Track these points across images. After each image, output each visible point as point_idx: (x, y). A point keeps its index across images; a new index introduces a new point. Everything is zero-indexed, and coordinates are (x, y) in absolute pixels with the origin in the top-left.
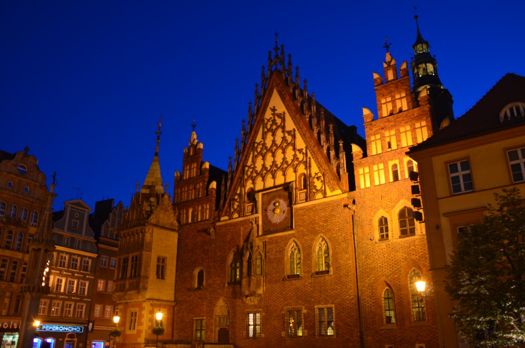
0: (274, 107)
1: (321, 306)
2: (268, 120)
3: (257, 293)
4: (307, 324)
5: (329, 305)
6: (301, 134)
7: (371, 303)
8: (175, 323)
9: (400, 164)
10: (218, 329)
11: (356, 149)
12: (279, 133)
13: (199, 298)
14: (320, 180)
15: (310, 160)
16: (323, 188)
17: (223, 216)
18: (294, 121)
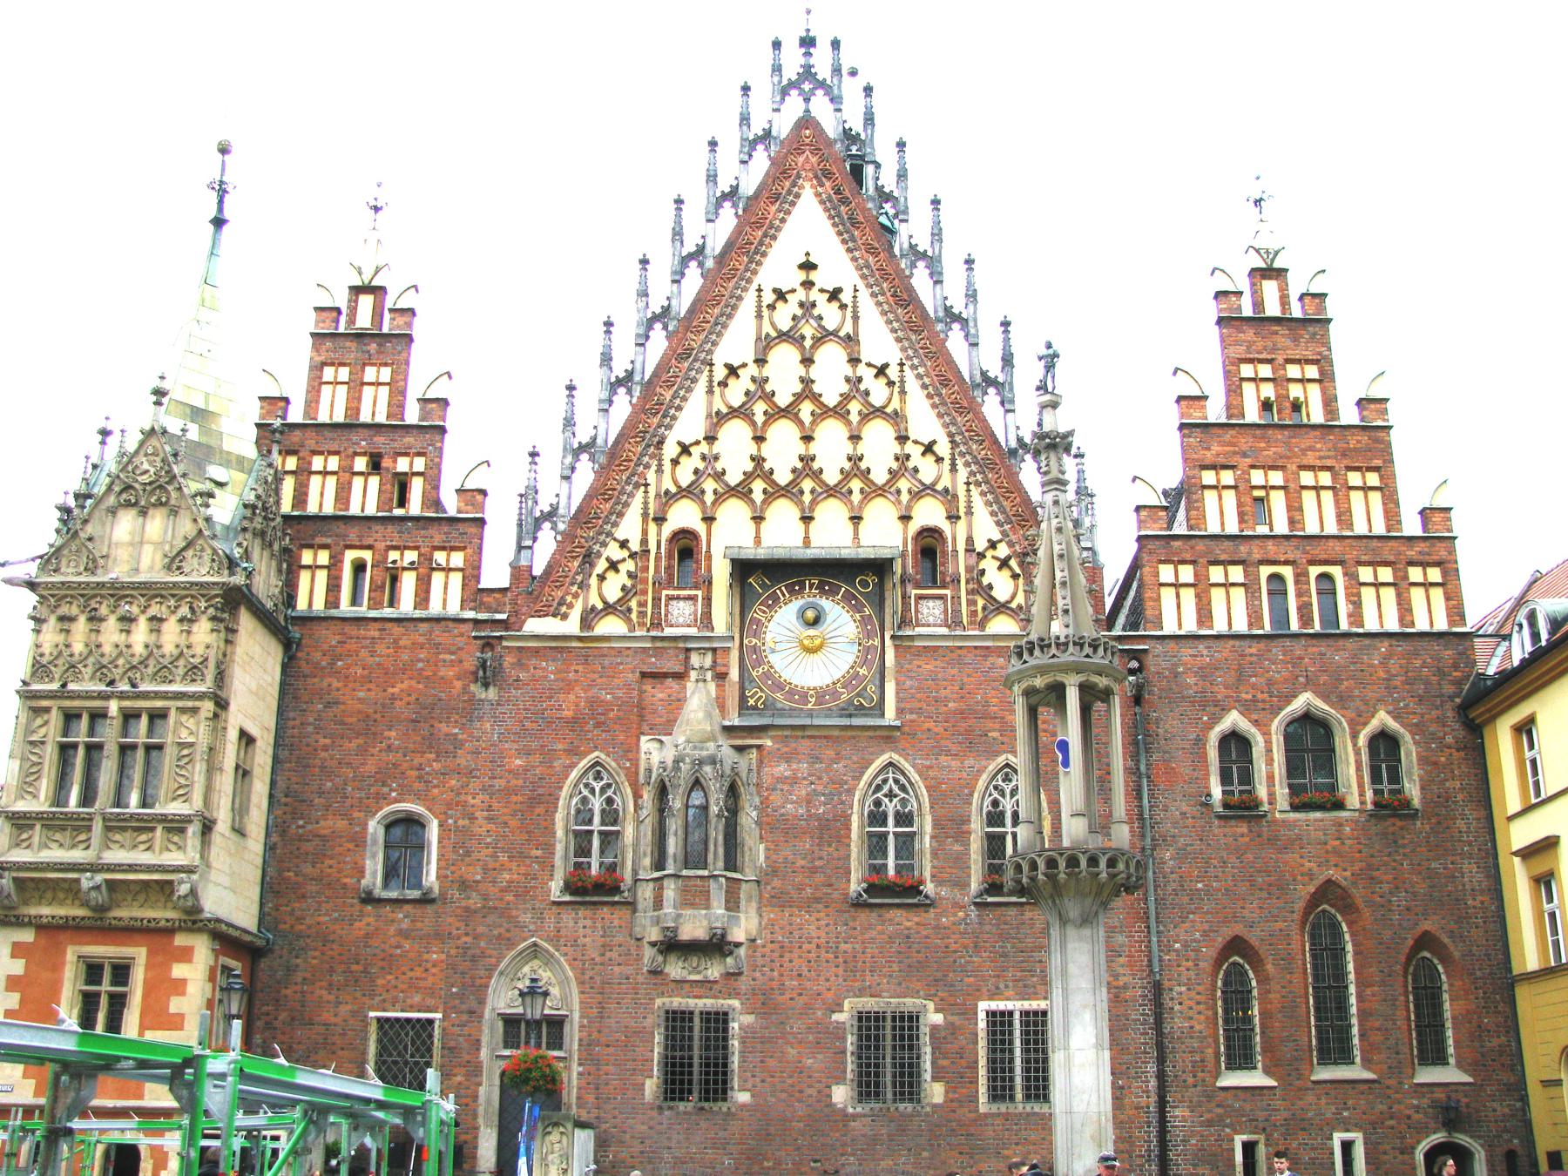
0: (808, 254)
2: (781, 295)
3: (729, 938)
4: (945, 1063)
6: (924, 386)
7: (1191, 1003)
8: (259, 1024)
9: (1297, 582)
10: (502, 1064)
12: (831, 358)
13: (404, 934)
14: (1006, 573)
15: (968, 490)
16: (1020, 599)
17: (539, 614)
18: (894, 331)
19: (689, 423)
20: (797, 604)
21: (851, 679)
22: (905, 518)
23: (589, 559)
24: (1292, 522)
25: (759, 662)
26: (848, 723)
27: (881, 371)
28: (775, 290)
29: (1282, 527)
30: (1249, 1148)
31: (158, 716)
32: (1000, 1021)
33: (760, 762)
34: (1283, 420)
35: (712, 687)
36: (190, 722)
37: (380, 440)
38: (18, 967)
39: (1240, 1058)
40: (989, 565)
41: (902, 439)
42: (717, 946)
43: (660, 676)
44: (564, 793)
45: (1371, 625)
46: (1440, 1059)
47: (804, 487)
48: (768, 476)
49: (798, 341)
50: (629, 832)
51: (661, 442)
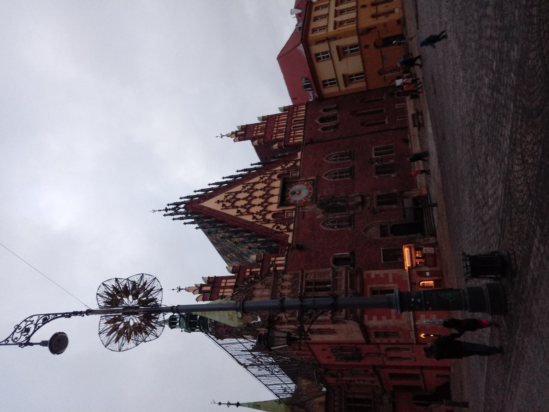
1: (373, 154)
2: (224, 205)
5: (373, 149)
10: (392, 235)
11: (276, 146)
17: (288, 240)
19: (249, 218)
20: (291, 196)
21: (307, 185)
22: (275, 180)
23: (276, 232)
24: (283, 126)
25: (302, 201)
26: (316, 185)
27: (244, 187)
28: (222, 207)
29: (285, 127)
30: (399, 118)
31: (308, 283)
32: (376, 154)
33: (323, 197)
34: (265, 129)
35: (307, 207)
36: (309, 276)
37: (240, 279)
38: (375, 318)
39: (384, 123)
40: (286, 167)
41: (258, 183)
42: (363, 197)
43: (304, 217)
44: (328, 230)
45: (304, 114)
46: (382, 99)
47: (267, 197)
48: (263, 203)
49: (235, 202)
50: (337, 217)
51: (252, 222)
